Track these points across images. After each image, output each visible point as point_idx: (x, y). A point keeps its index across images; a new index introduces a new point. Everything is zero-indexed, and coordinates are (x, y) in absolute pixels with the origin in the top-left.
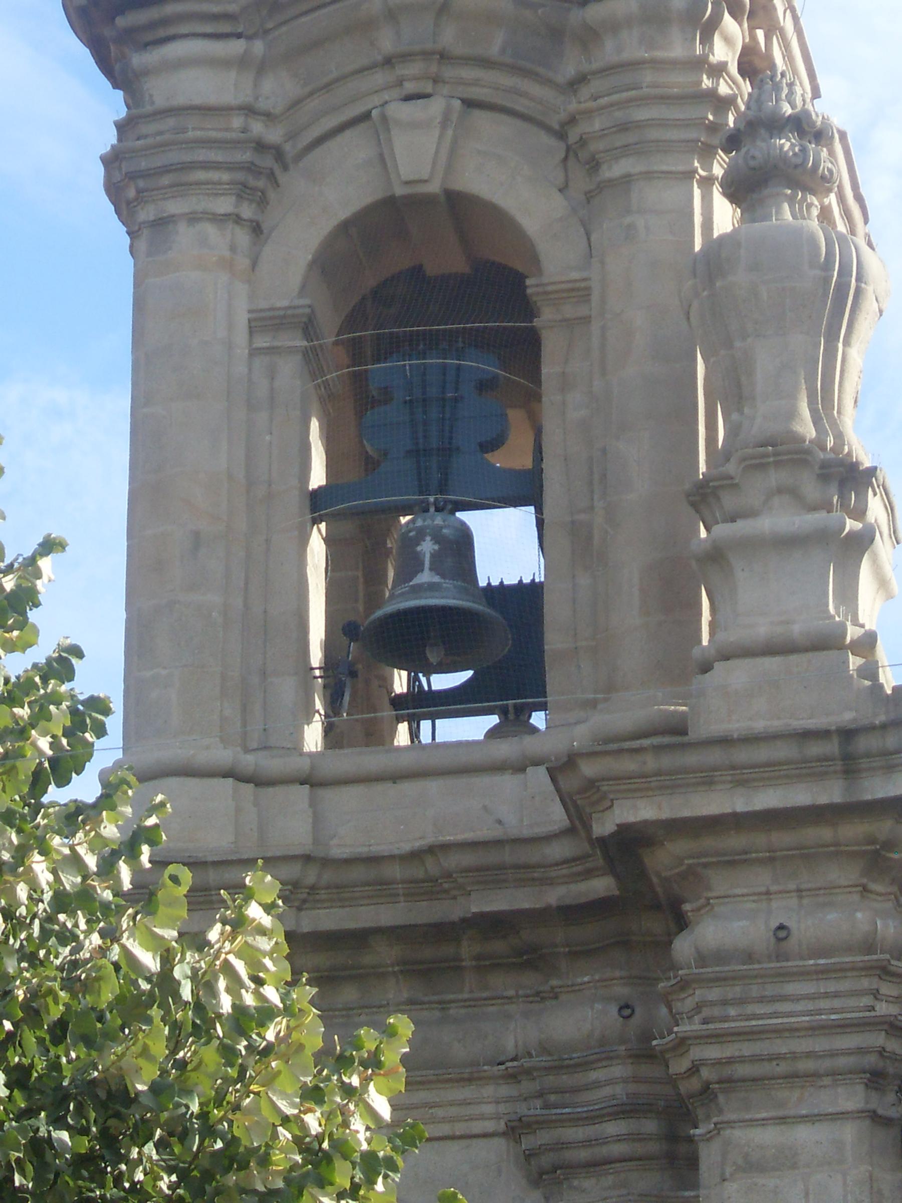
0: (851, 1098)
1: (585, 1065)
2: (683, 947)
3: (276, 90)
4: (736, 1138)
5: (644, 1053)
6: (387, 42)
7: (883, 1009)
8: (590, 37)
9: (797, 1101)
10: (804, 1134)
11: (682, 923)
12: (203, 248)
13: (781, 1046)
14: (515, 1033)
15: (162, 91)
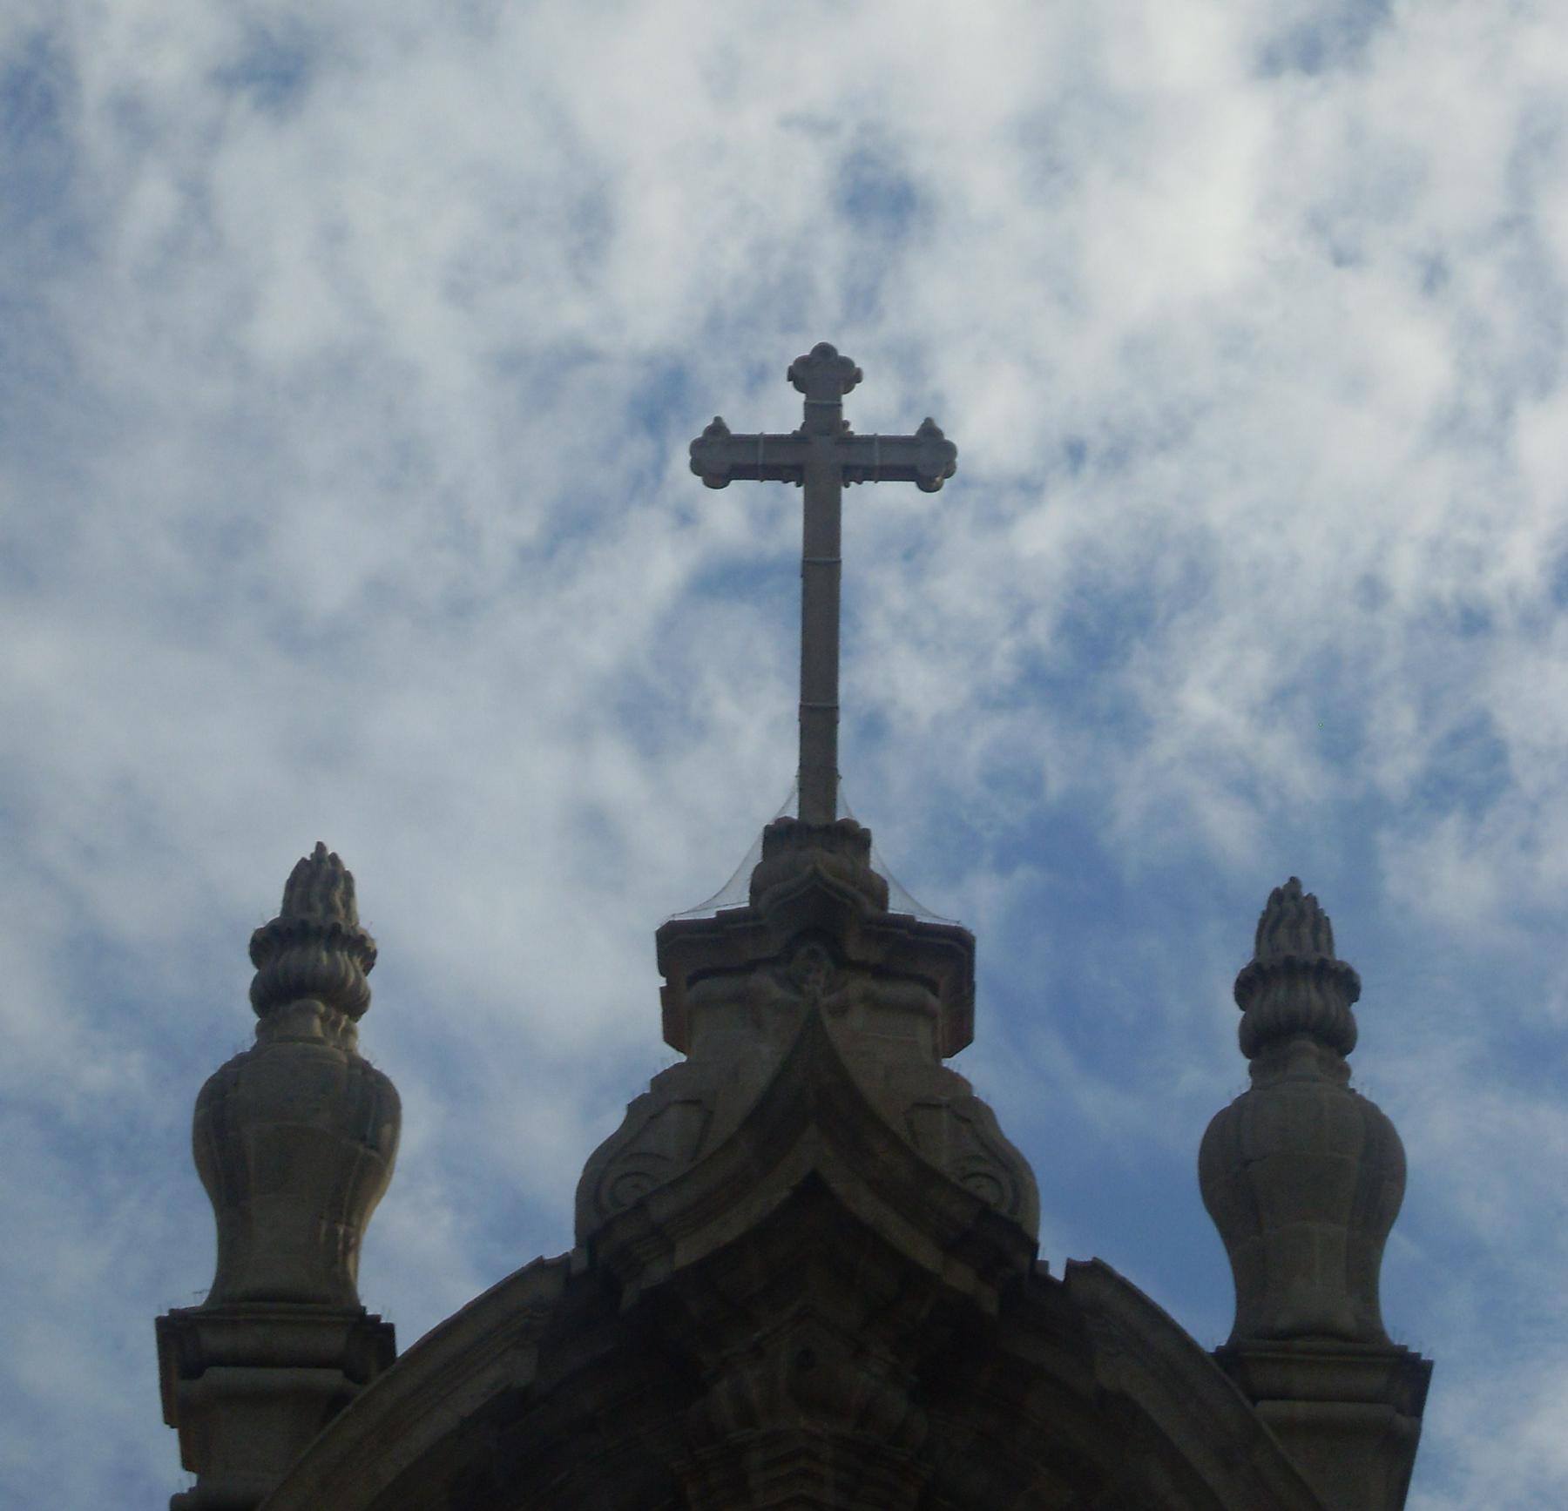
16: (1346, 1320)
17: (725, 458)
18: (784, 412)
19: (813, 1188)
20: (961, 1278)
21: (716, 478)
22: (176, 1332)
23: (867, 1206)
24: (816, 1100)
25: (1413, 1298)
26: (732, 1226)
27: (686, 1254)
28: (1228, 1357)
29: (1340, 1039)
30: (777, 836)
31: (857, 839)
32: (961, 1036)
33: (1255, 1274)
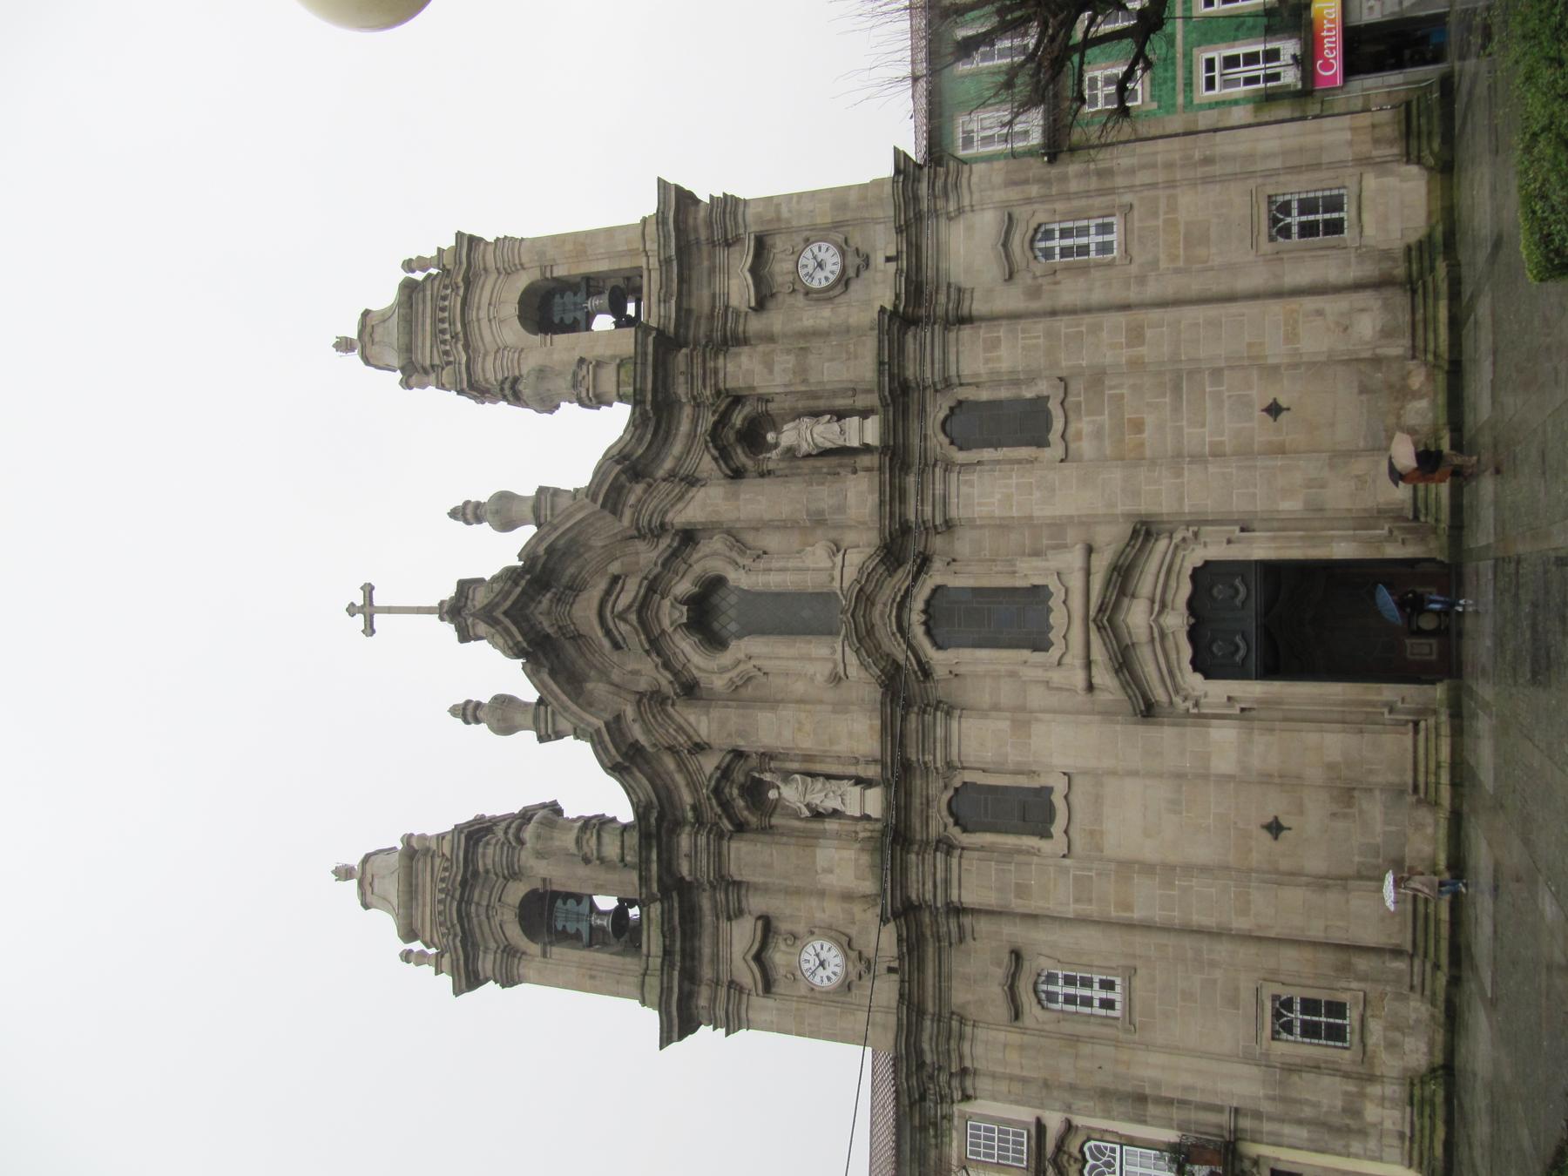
0: (725, 843)
2: (688, 878)
3: (492, 945)
4: (735, 871)
6: (483, 917)
8: (487, 872)
11: (682, 879)
12: (526, 968)
14: (708, 918)
15: (489, 973)
16: (530, 503)
17: (369, 630)
18: (360, 617)
19: (506, 613)
20: (523, 583)
21: (373, 632)
22: (541, 739)
23: (509, 603)
24: (488, 615)
25: (526, 489)
26: (514, 629)
27: (520, 638)
28: (539, 526)
29: (478, 505)
30: (442, 619)
31: (442, 603)
32: (481, 581)
33: (523, 522)
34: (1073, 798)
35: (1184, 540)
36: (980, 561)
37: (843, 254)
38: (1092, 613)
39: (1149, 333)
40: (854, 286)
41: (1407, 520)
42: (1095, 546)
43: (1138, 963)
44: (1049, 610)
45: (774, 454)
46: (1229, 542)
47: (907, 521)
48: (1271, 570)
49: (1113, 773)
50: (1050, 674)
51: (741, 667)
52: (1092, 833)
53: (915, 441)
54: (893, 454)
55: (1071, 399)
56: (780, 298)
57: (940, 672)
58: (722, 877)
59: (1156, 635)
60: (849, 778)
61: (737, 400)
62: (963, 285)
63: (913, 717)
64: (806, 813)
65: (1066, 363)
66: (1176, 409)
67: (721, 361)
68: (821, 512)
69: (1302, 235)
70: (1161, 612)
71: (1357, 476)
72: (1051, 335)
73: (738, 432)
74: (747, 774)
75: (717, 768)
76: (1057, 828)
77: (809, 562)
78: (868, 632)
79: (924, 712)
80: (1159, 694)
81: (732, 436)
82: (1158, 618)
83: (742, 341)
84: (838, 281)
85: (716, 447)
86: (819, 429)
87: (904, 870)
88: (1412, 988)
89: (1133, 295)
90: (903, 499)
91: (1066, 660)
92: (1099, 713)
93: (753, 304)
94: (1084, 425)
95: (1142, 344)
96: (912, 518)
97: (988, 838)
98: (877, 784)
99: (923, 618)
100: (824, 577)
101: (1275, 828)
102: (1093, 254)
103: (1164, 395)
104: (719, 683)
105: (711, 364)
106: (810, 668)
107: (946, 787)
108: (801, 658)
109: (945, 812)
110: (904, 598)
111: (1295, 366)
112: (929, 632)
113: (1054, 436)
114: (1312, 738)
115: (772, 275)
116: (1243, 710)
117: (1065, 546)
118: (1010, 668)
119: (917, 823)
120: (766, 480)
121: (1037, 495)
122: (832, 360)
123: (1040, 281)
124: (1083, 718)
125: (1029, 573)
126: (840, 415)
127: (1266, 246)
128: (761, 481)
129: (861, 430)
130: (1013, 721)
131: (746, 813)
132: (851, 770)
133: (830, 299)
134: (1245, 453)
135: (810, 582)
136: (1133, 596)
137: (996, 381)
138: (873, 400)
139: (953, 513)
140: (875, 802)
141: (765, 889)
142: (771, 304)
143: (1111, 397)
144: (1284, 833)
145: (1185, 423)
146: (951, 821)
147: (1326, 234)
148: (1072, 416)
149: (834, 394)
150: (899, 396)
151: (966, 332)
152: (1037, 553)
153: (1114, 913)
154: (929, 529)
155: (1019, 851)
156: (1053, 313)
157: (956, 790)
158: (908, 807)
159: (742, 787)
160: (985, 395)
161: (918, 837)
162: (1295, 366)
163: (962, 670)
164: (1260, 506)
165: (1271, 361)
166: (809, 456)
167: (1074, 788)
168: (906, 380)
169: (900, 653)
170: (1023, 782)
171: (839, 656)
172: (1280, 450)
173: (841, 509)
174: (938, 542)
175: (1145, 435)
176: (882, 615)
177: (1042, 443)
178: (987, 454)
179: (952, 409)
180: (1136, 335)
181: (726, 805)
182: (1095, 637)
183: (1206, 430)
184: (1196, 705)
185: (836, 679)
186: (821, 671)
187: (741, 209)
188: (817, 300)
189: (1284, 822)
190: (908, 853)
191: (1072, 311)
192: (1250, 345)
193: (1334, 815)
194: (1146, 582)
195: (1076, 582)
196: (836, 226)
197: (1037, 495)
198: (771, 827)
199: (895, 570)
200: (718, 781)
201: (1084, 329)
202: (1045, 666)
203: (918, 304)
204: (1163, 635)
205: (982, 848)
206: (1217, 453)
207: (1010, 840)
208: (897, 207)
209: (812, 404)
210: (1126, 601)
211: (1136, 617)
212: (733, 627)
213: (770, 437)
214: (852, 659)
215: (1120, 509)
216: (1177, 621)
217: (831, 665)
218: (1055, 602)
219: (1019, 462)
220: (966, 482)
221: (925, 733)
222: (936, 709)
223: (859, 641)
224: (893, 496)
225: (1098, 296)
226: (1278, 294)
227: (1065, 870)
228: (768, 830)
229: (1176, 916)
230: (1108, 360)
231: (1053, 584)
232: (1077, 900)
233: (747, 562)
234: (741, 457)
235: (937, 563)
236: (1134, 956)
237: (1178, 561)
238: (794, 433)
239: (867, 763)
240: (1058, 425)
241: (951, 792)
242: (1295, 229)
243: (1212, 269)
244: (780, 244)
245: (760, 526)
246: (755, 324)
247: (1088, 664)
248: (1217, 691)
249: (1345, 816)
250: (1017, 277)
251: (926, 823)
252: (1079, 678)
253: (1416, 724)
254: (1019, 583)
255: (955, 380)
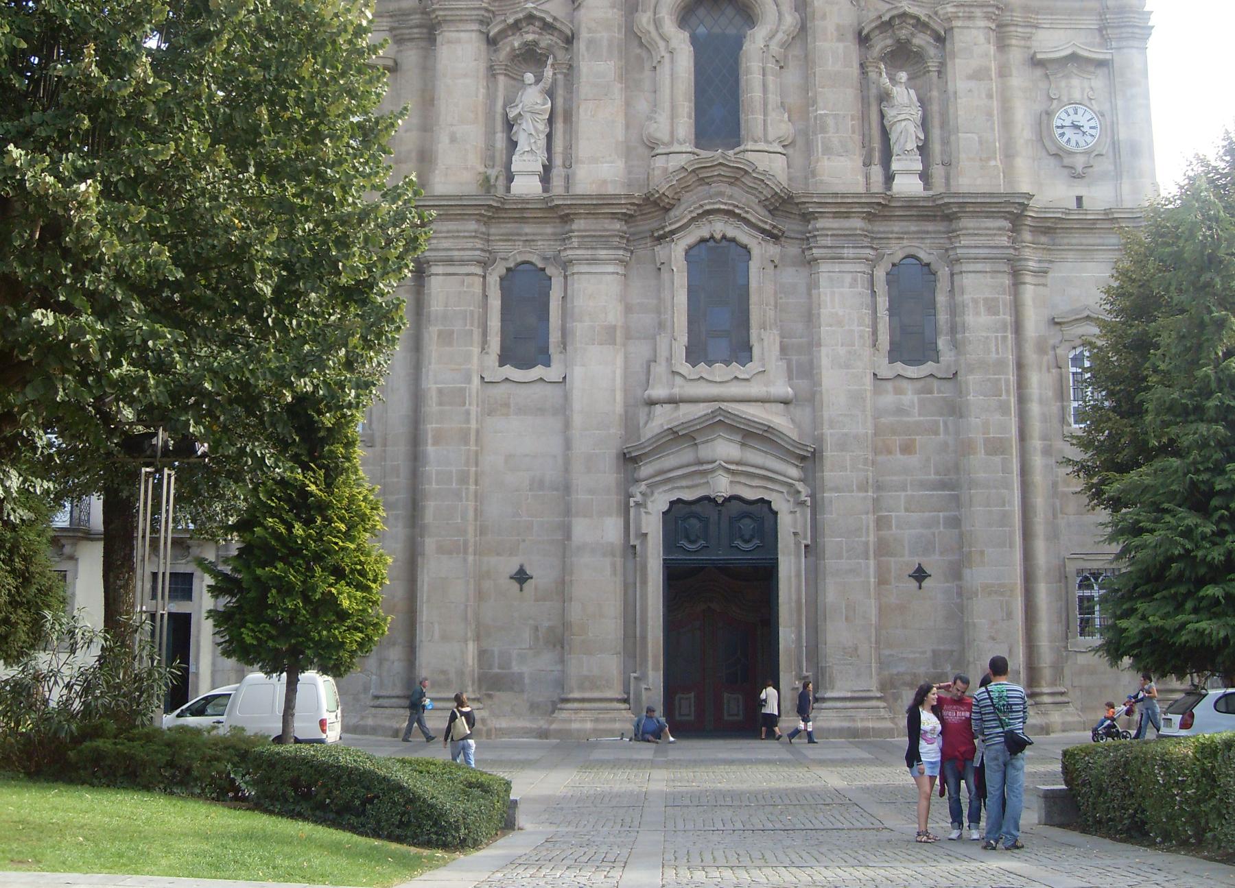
0: (475, 27)
1: (409, 15)
4: (446, 35)
5: (424, 13)
7: (484, 5)
9: (462, 26)
10: (462, 35)
13: (459, 13)
34: (538, 388)
35: (799, 492)
36: (776, 293)
37: (1087, 153)
38: (724, 406)
39: (997, 459)
40: (1052, 162)
41: (816, 689)
42: (791, 407)
43: (378, 448)
44: (727, 363)
45: (885, 80)
46: (795, 534)
47: (816, 218)
48: (767, 574)
49: (567, 425)
50: (664, 363)
51: (662, 44)
52: (507, 405)
53: (897, 227)
54: (884, 206)
55: (936, 383)
56: (1043, 85)
57: (661, 251)
58: (439, 23)
59: (705, 467)
60: (550, 159)
61: (940, 39)
62: (1050, 275)
63: (618, 225)
64: (512, 114)
65: (972, 380)
66: (923, 485)
67: (982, 23)
68: (824, 129)
69: (1081, 599)
70: (728, 470)
71: (856, 649)
72: (1000, 365)
73: (908, 41)
74: (549, 49)
75: (555, 19)
76: (509, 371)
77: (773, 116)
78: (702, 179)
79: (622, 237)
80: (645, 470)
81: (903, 34)
82: (726, 471)
83: (1002, 46)
84: (1061, 148)
85: (892, 18)
86: (912, 128)
87: (462, 217)
88: (377, 697)
89: (1036, 443)
90: (836, 215)
91: (678, 380)
92: (626, 412)
93: (1039, 56)
94: (910, 397)
95: (987, 453)
96: (820, 224)
97: (495, 303)
98: (545, 190)
99: (718, 236)
100: (759, 131)
101: (521, 577)
102: (1075, 404)
103: (937, 473)
104: (644, 19)
105: (978, 12)
106: (663, 119)
107: (545, 259)
108: (673, 108)
109: (519, 259)
110: (738, 216)
111: (960, 594)
112: (703, 241)
113: (899, 367)
114: (613, 608)
115: (1067, 77)
116: (634, 547)
117: (790, 378)
118: (669, 324)
119: (510, 227)
120: (855, 70)
121: (842, 351)
122: (980, 142)
123: (1051, 353)
124: (619, 396)
125: (765, 343)
126: (923, 149)
127: (1072, 567)
128: (856, 65)
129: (908, 172)
130: (614, 328)
131: (508, 49)
132: (558, 160)
133: (1040, 139)
134: (883, 549)
135: (753, 120)
136: (743, 445)
137: (954, 310)
138: (939, 187)
139: (824, 267)
140: (527, 186)
141: (428, 69)
142: (1039, 72)
143: (936, 422)
144: (516, 586)
145: (909, 493)
146: (512, 265)
147: (1082, 620)
148: (919, 384)
149: (945, 142)
150: (941, 213)
151: (1007, 281)
152: (784, 350)
153: (430, 427)
154: (807, 240)
155: (485, 334)
156: (1020, 366)
157: (543, 270)
158: (523, 220)
159: (535, 43)
160: (941, 299)
161: (493, 231)
162: (960, 594)
163: (665, 275)
164: (830, 563)
165: (967, 573)
166: (882, 116)
167: (549, 387)
168: (959, 218)
169: (681, 214)
170: (554, 337)
171: (676, 148)
172: (882, 581)
173: (828, 150)
174: (793, 250)
175: (899, 456)
176: (722, 194)
177: (896, 354)
178: (883, 302)
179: (928, 265)
180: (996, 447)
181: (516, 26)
182: (702, 410)
183: (902, 513)
184: (637, 504)
185: (651, 146)
186: (660, 127)
187: (1136, 44)
188: (1040, 124)
189: (528, 585)
190: (478, 221)
191: (1021, 384)
192: (982, 553)
193: (536, 629)
194: (756, 457)
195: (755, 389)
196: (1115, 145)
197: (842, 351)
198: (494, 76)
199: (765, 206)
200: (543, 20)
201: (1004, 397)
202: (669, 360)
203: (1036, 230)
204: (704, 473)
205: (485, 297)
206: (881, 523)
207: (495, 323)
208: (1131, 210)
209: (936, 122)
210: (738, 438)
211: (725, 449)
212: (701, 30)
213: (903, 76)
214: (675, 162)
215: (827, 431)
216: (722, 486)
217: (666, 138)
218: (736, 369)
219: (875, 333)
220: (855, 280)
221: (602, 240)
222: (625, 249)
223: (693, 171)
224: (842, 207)
225: (1035, 409)
226: (1029, 578)
227: (468, 380)
228: (492, 73)
229: (432, 486)
230: (973, 420)
231: (754, 367)
232: (440, 391)
233: (774, 47)
234: (882, 43)
235: (773, 250)
236: (385, 445)
237: (777, 487)
238: (906, 101)
239: (567, 178)
240: (911, 371)
241: (540, 266)
242: (1087, 593)
243: (1055, 516)
244: (1098, 82)
245: (807, 62)
246: (1016, 56)
247: (674, 401)
248: (652, 525)
249: (537, 638)
250: (1058, 327)
251: (507, 238)
252: (659, 392)
253: (626, 701)
254: (754, 333)
255: (957, 268)
